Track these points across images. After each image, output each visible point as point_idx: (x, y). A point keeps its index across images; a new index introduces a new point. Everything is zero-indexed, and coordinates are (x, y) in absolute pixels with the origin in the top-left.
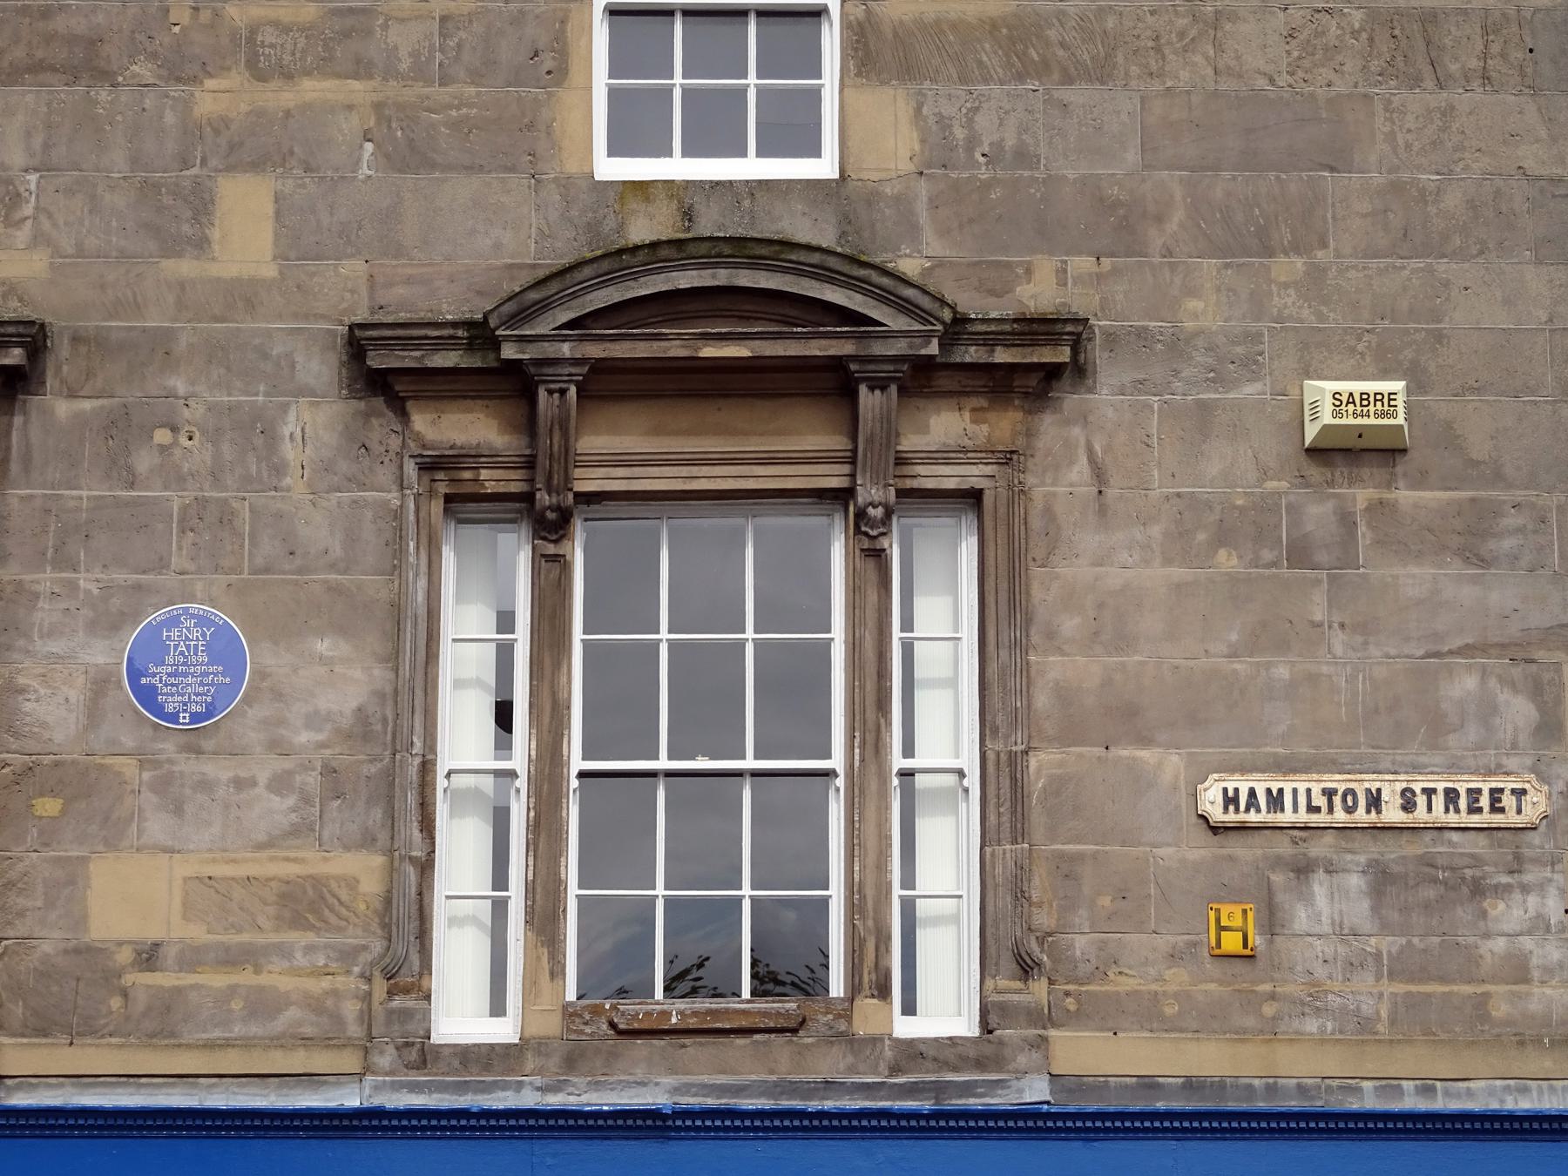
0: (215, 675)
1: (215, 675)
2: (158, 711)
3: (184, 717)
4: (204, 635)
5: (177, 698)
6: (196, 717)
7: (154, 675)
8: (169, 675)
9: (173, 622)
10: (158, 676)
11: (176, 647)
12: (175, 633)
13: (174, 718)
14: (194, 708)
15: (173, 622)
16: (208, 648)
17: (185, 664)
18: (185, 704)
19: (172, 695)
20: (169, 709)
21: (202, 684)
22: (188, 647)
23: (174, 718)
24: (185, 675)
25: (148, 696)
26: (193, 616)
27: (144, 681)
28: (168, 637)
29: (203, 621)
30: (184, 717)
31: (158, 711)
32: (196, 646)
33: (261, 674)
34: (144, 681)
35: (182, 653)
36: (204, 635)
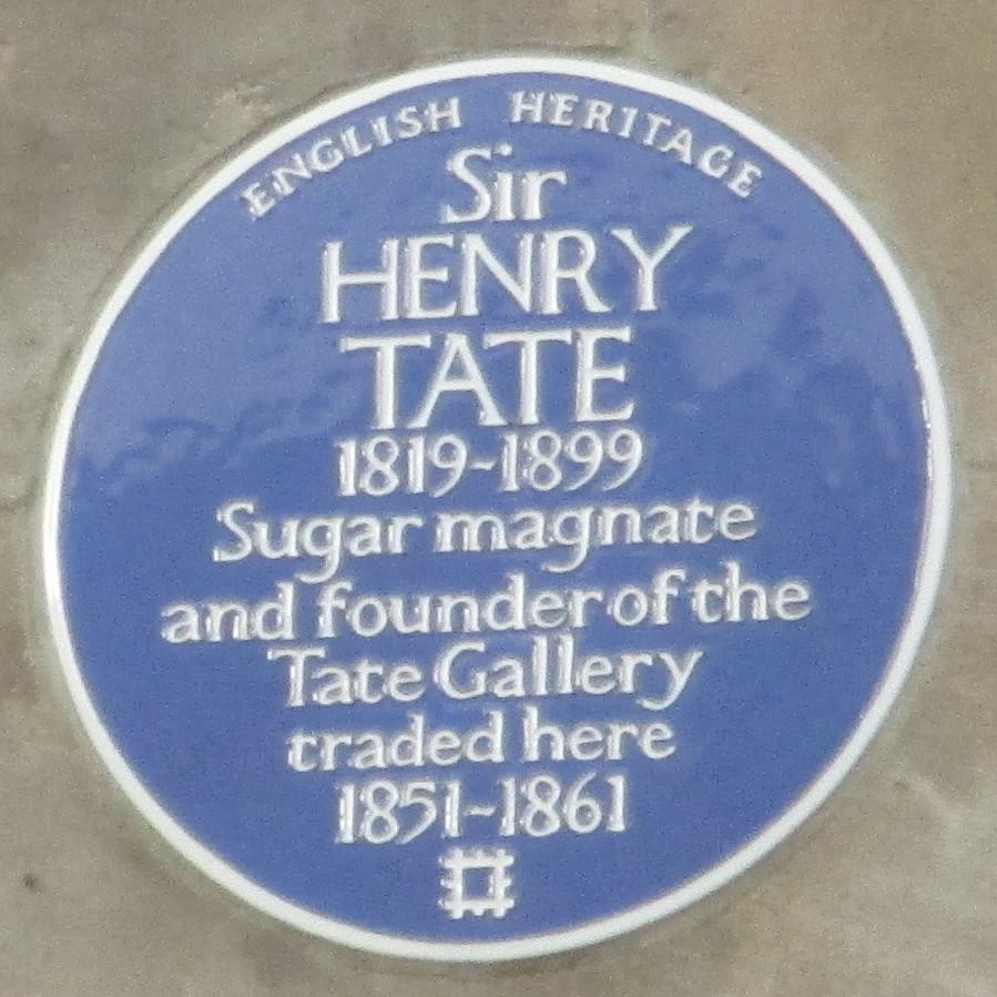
0: (705, 559)
1: (705, 559)
2: (281, 828)
3: (478, 882)
4: (616, 276)
5: (423, 743)
6: (562, 878)
7: (256, 580)
8: (371, 574)
9: (394, 191)
11: (416, 371)
12: (402, 274)
13: (397, 885)
14: (552, 810)
15: (394, 191)
16: (656, 371)
17: (480, 492)
18: (481, 782)
19: (390, 718)
20: (359, 818)
21: (602, 636)
22: (502, 370)
23: (397, 885)
24: (482, 572)
26: (538, 146)
27: (187, 624)
28: (363, 309)
30: (478, 882)
31: (281, 828)
32: (559, 364)
34: (187, 624)
35: (459, 412)
36: (616, 276)
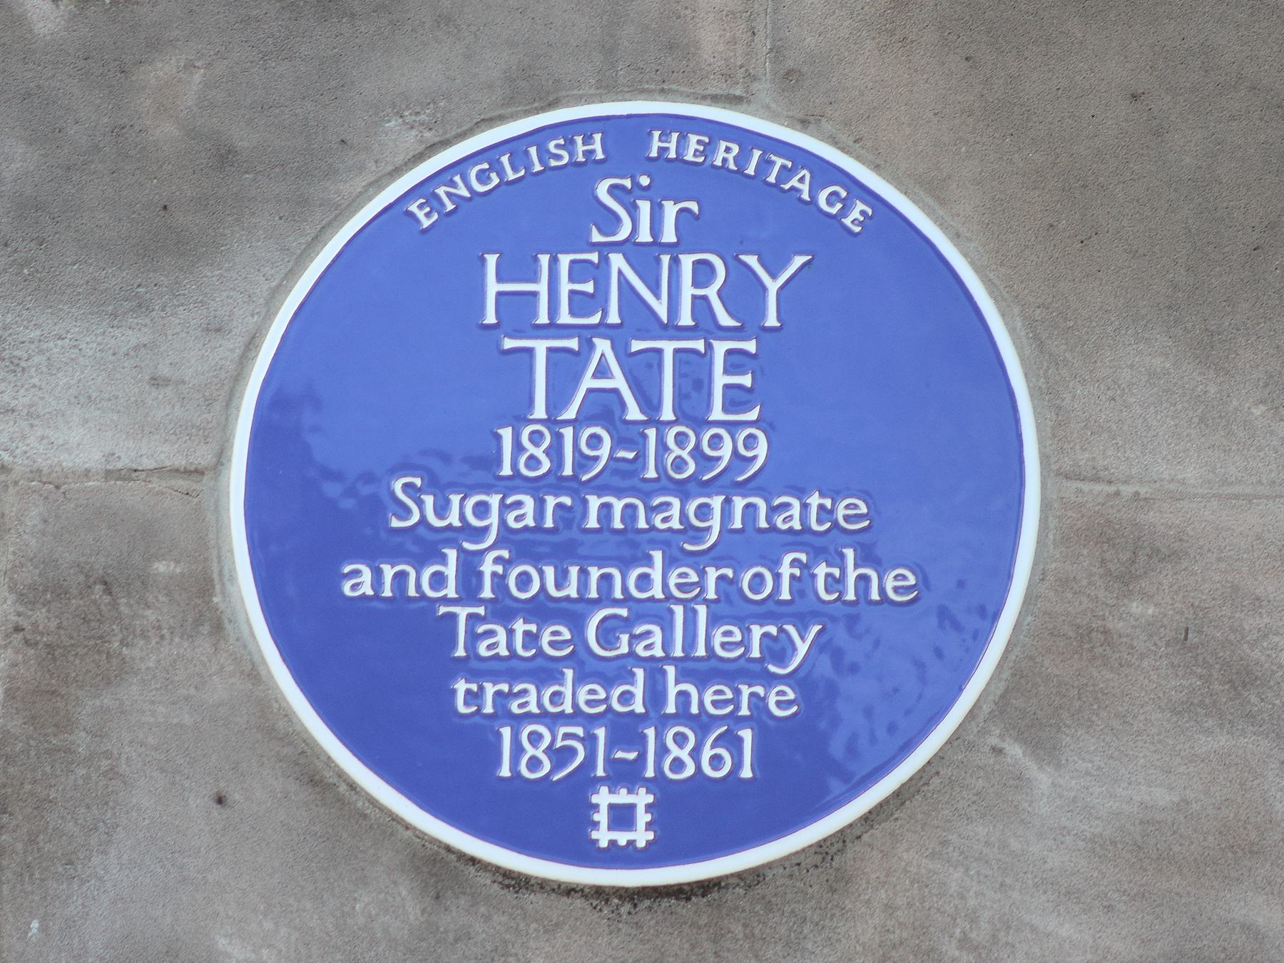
0: (820, 546)
1: (820, 546)
4: (744, 293)
5: (573, 693)
6: (693, 816)
7: (424, 545)
8: (525, 546)
9: (541, 208)
10: (455, 550)
11: (566, 368)
12: (553, 284)
13: (552, 815)
15: (541, 208)
16: (776, 378)
17: (622, 477)
18: (626, 730)
19: (544, 672)
20: (524, 756)
21: (730, 608)
22: (643, 374)
23: (552, 815)
24: (629, 547)
25: (387, 680)
26: (674, 177)
27: (360, 581)
29: (740, 207)
30: (621, 814)
31: (451, 767)
32: (694, 374)
33: (1113, 546)
34: (360, 581)
35: (603, 409)
36: (744, 293)
